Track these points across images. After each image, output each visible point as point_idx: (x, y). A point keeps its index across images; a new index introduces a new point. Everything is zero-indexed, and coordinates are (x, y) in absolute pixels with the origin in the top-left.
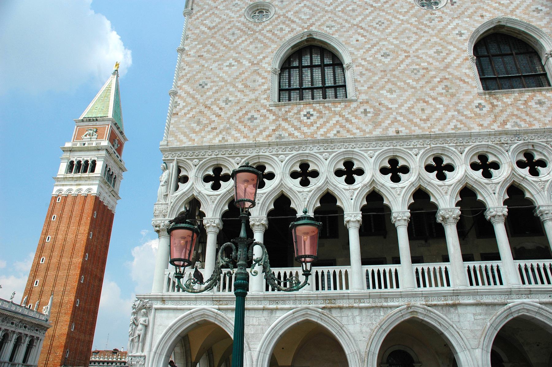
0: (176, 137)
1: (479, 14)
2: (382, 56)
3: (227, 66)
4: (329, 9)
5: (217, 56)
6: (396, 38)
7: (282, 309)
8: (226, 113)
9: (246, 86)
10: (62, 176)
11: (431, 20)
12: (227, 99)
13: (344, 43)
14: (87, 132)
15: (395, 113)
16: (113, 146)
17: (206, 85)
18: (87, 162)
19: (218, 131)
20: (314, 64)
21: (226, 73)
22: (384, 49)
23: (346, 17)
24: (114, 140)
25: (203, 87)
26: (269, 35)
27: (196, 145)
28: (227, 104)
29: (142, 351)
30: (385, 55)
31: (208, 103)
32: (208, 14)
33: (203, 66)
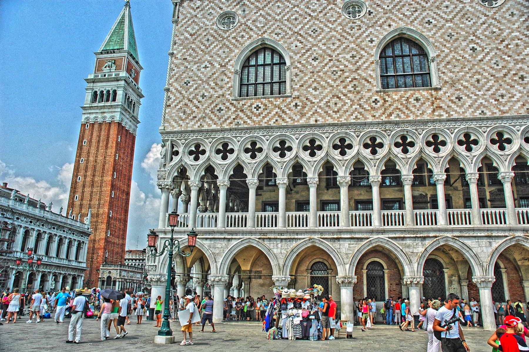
0: (170, 123)
1: (387, 24)
2: (313, 60)
3: (203, 68)
4: (278, 18)
5: (197, 60)
6: (324, 44)
7: (235, 239)
8: (203, 106)
9: (216, 84)
11: (352, 28)
12: (203, 94)
13: (286, 49)
14: (106, 64)
15: (316, 107)
16: (131, 75)
17: (189, 83)
18: (108, 92)
19: (197, 119)
20: (266, 63)
22: (315, 54)
23: (290, 26)
24: (131, 70)
25: (187, 85)
26: (233, 41)
27: (183, 129)
28: (203, 98)
30: (315, 59)
31: (191, 97)
32: (190, 22)
33: (187, 67)
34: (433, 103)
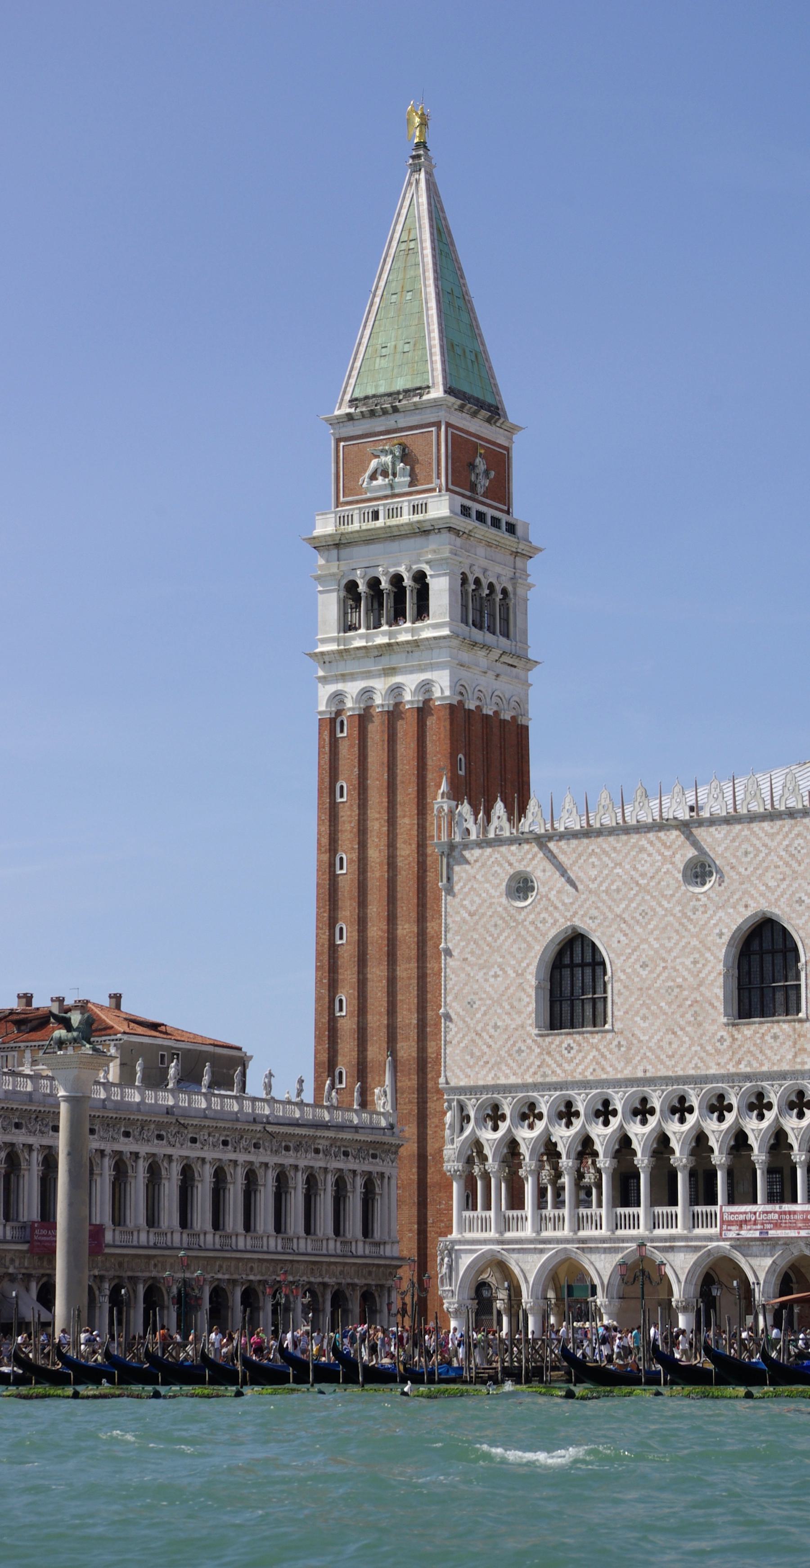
1: (743, 903)
4: (592, 886)
5: (481, 961)
6: (657, 939)
9: (512, 1007)
10: (333, 647)
11: (695, 910)
12: (496, 1024)
14: (374, 463)
17: (475, 1003)
18: (397, 579)
19: (490, 1065)
21: (492, 986)
24: (472, 466)
25: (472, 1006)
26: (532, 929)
29: (451, 1285)
30: (644, 966)
31: (479, 1028)
32: (466, 890)
33: (469, 975)
34: (795, 1043)
